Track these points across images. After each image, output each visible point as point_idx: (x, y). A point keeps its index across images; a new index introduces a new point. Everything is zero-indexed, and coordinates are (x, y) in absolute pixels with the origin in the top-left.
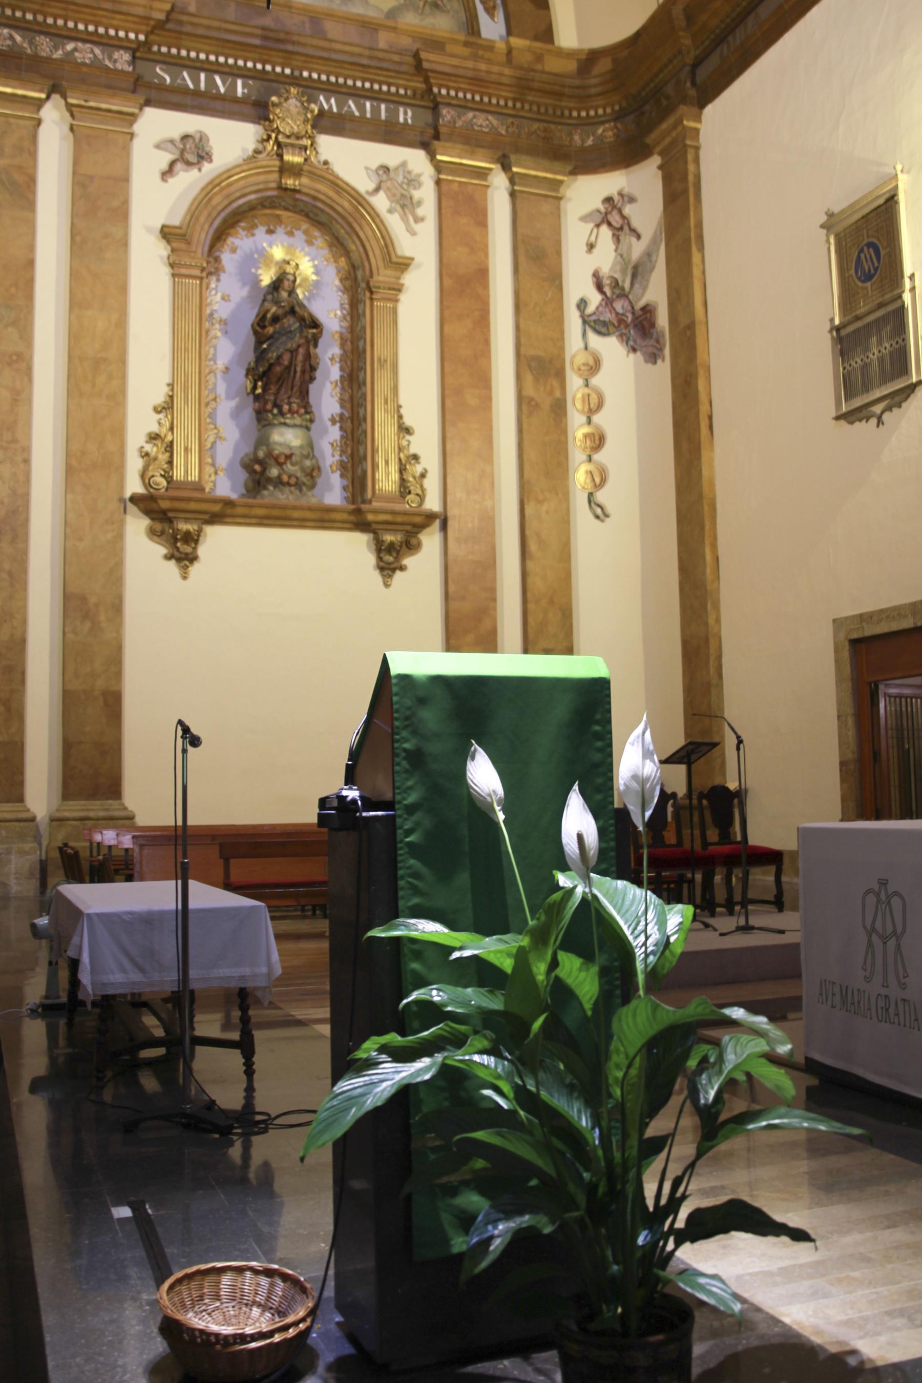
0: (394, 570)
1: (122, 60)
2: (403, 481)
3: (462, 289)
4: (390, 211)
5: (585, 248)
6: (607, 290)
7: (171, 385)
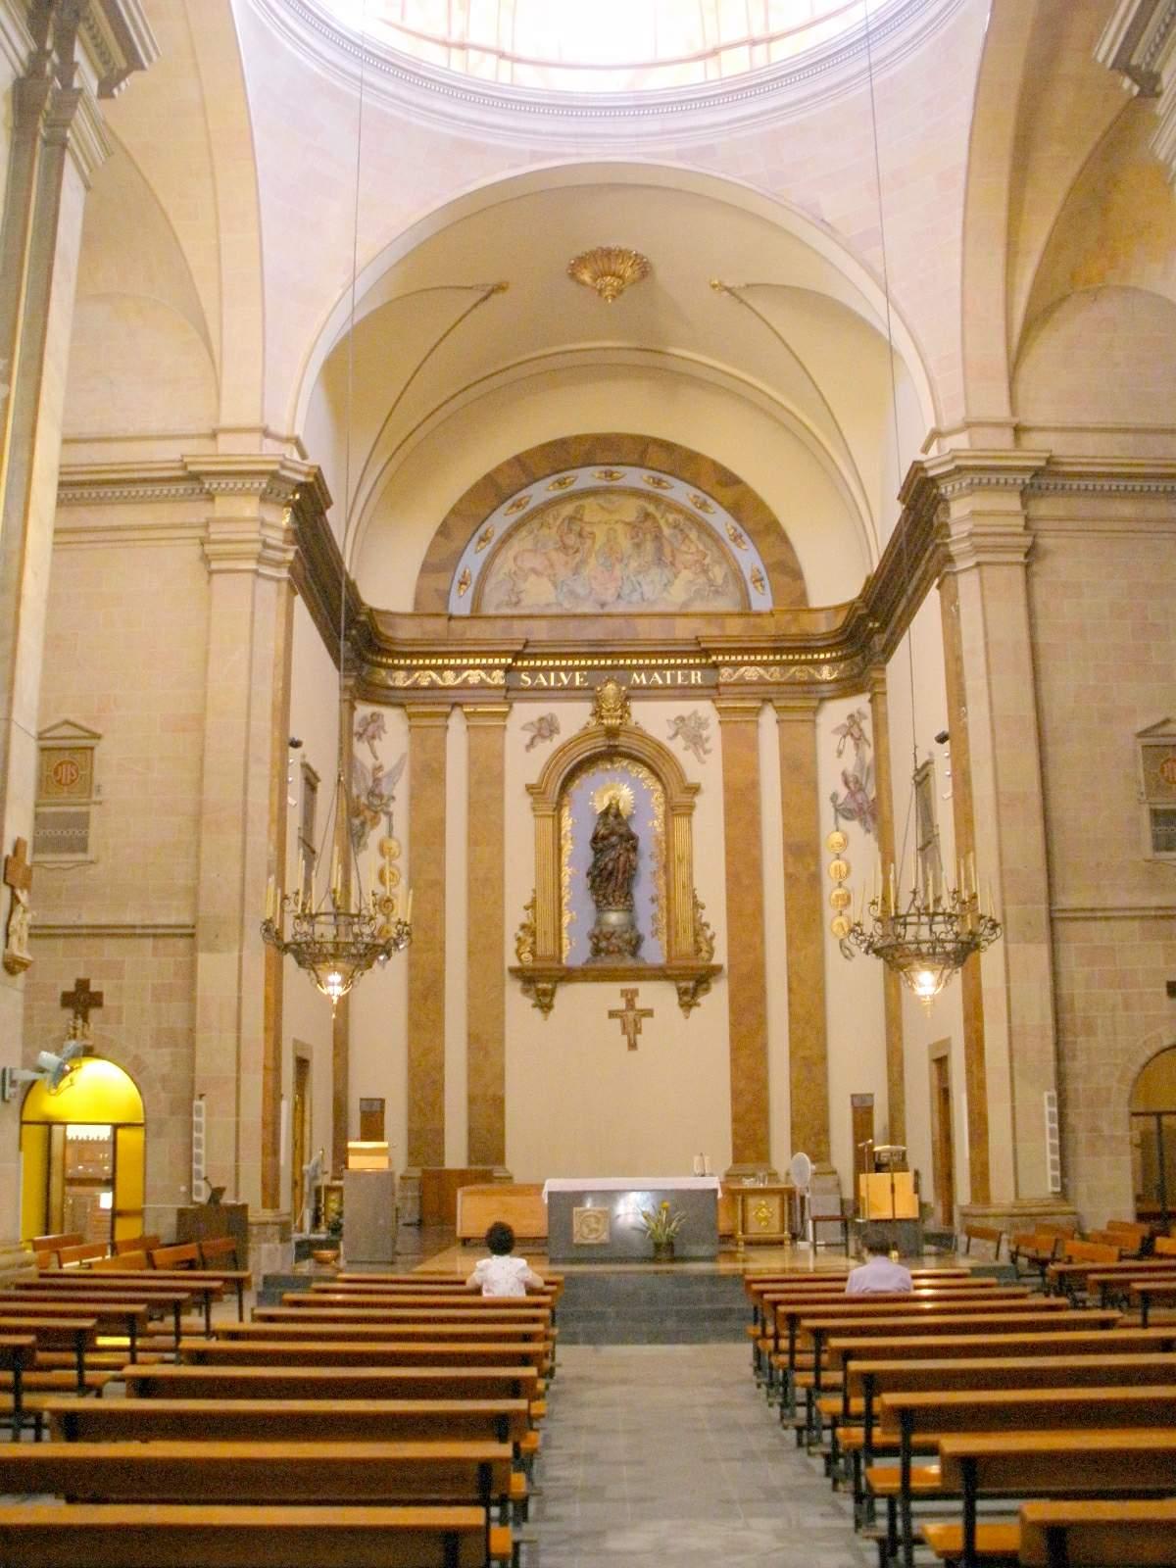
0: (690, 1006)
1: (498, 678)
2: (696, 941)
3: (741, 801)
4: (686, 749)
5: (836, 754)
6: (852, 785)
7: (534, 891)
